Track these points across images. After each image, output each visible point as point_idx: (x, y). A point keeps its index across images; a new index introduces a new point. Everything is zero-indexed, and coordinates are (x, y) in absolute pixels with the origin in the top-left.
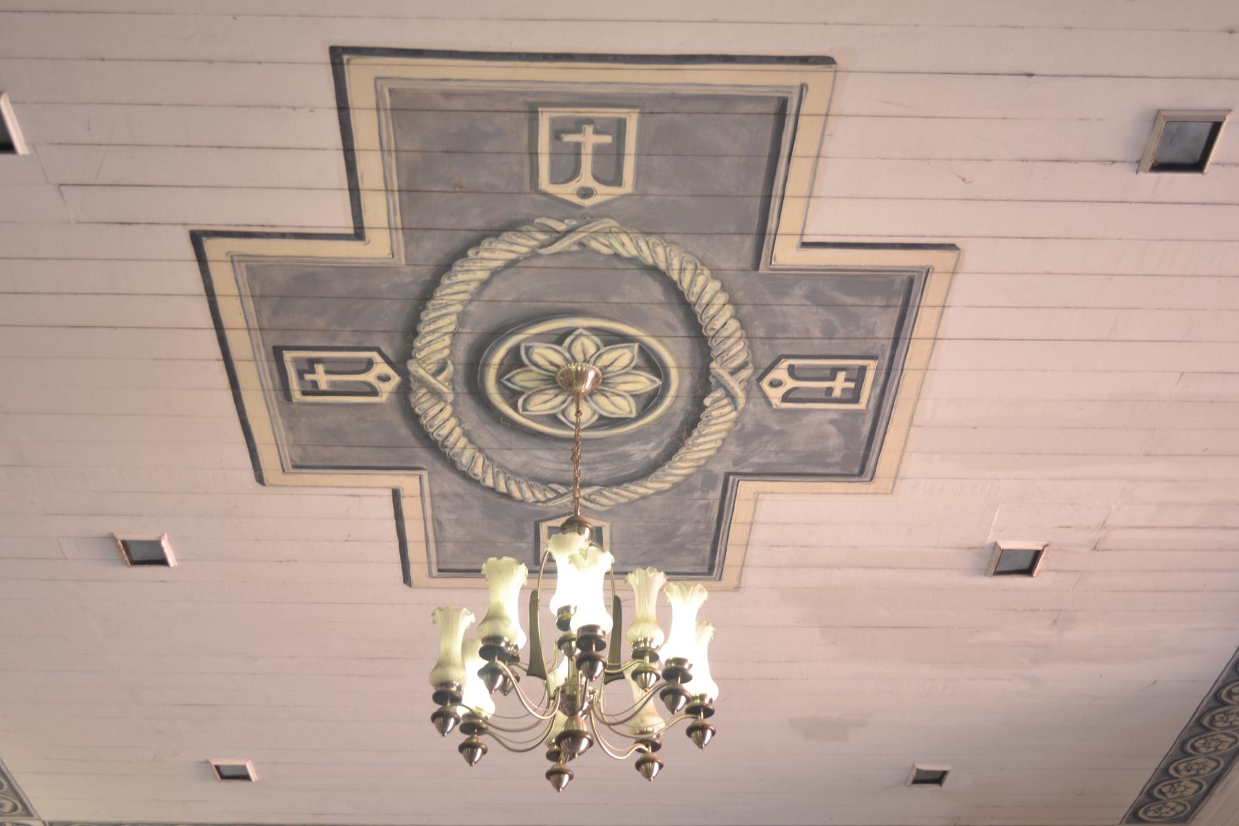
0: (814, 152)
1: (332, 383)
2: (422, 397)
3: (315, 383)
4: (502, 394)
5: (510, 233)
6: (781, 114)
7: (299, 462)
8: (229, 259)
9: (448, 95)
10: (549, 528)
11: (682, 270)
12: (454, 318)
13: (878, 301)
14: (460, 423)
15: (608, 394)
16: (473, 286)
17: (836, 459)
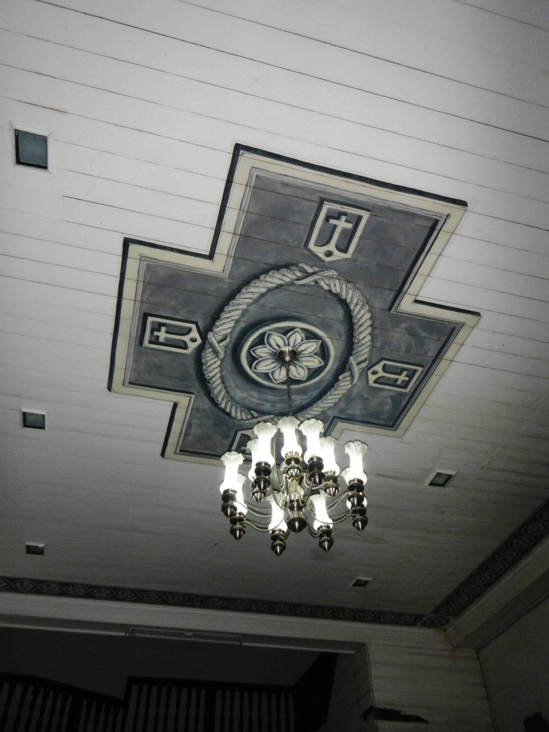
0: (439, 253)
1: (166, 339)
2: (209, 353)
3: (158, 337)
4: (247, 358)
5: (285, 269)
6: (432, 229)
7: (133, 380)
8: (139, 258)
9: (285, 185)
10: (242, 435)
11: (357, 304)
12: (239, 312)
13: (436, 337)
14: (221, 372)
15: (297, 366)
16: (257, 295)
17: (385, 417)
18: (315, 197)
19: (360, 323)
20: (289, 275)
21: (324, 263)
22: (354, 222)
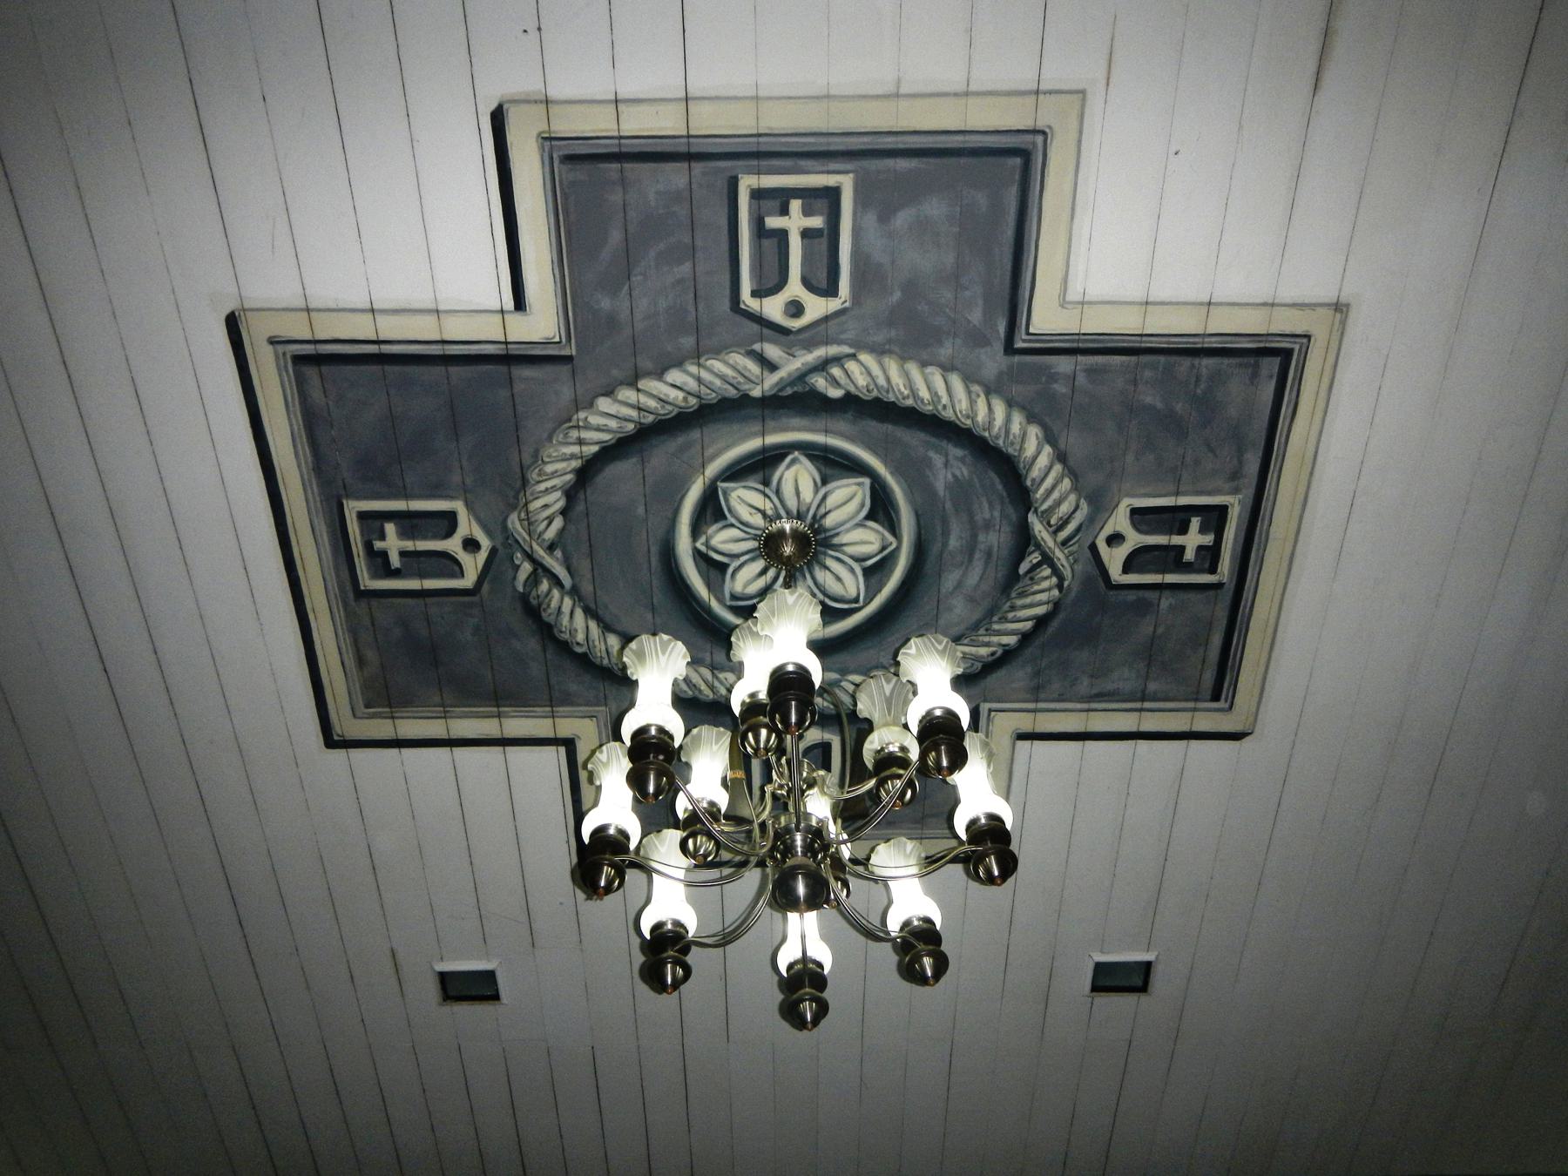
9: (361, 662)
11: (580, 442)
15: (822, 511)
18: (362, 608)
19: (634, 414)
20: (554, 604)
21: (499, 546)
22: (377, 524)
